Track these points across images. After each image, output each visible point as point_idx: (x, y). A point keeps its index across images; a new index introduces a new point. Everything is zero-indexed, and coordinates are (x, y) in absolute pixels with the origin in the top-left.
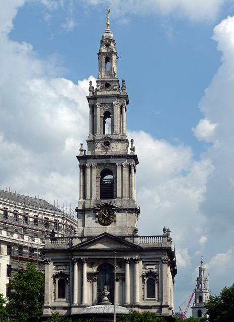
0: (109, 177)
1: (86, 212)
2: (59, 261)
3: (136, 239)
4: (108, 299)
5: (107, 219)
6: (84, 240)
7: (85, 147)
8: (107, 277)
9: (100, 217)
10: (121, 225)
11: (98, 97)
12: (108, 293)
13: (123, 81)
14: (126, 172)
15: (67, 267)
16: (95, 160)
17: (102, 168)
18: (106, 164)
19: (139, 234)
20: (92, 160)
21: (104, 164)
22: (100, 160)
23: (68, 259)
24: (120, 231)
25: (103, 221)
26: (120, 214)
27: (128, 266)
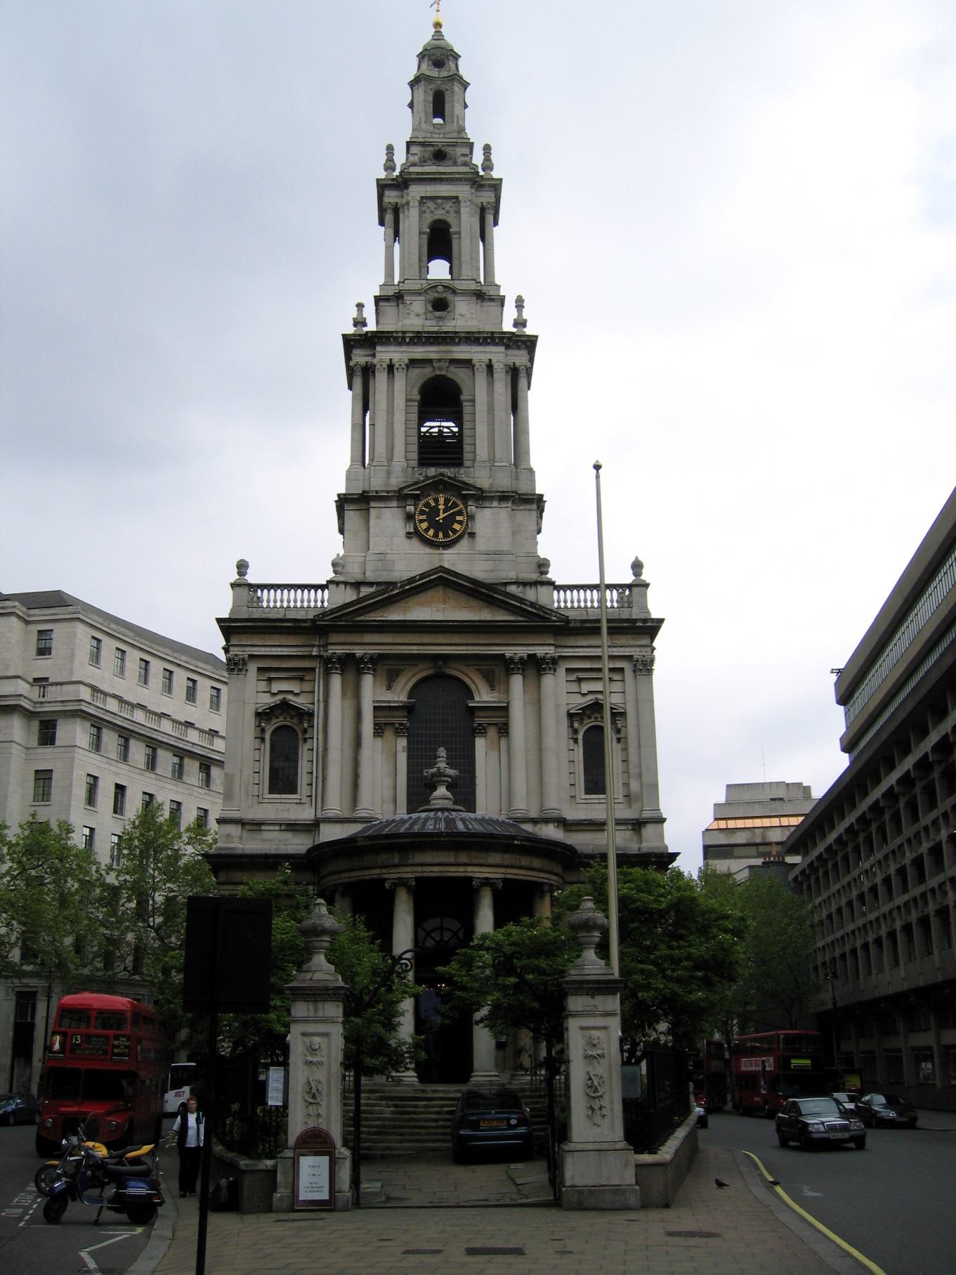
1: (372, 504)
2: (275, 664)
3: (543, 591)
4: (448, 794)
5: (445, 527)
6: (365, 591)
7: (370, 314)
9: (422, 521)
11: (413, 180)
12: (451, 772)
13: (487, 149)
15: (307, 686)
16: (404, 348)
17: (427, 372)
18: (440, 360)
19: (553, 575)
20: (392, 348)
21: (430, 361)
22: (421, 349)
23: (310, 657)
24: (488, 565)
25: (431, 532)
26: (487, 512)
27: (517, 682)
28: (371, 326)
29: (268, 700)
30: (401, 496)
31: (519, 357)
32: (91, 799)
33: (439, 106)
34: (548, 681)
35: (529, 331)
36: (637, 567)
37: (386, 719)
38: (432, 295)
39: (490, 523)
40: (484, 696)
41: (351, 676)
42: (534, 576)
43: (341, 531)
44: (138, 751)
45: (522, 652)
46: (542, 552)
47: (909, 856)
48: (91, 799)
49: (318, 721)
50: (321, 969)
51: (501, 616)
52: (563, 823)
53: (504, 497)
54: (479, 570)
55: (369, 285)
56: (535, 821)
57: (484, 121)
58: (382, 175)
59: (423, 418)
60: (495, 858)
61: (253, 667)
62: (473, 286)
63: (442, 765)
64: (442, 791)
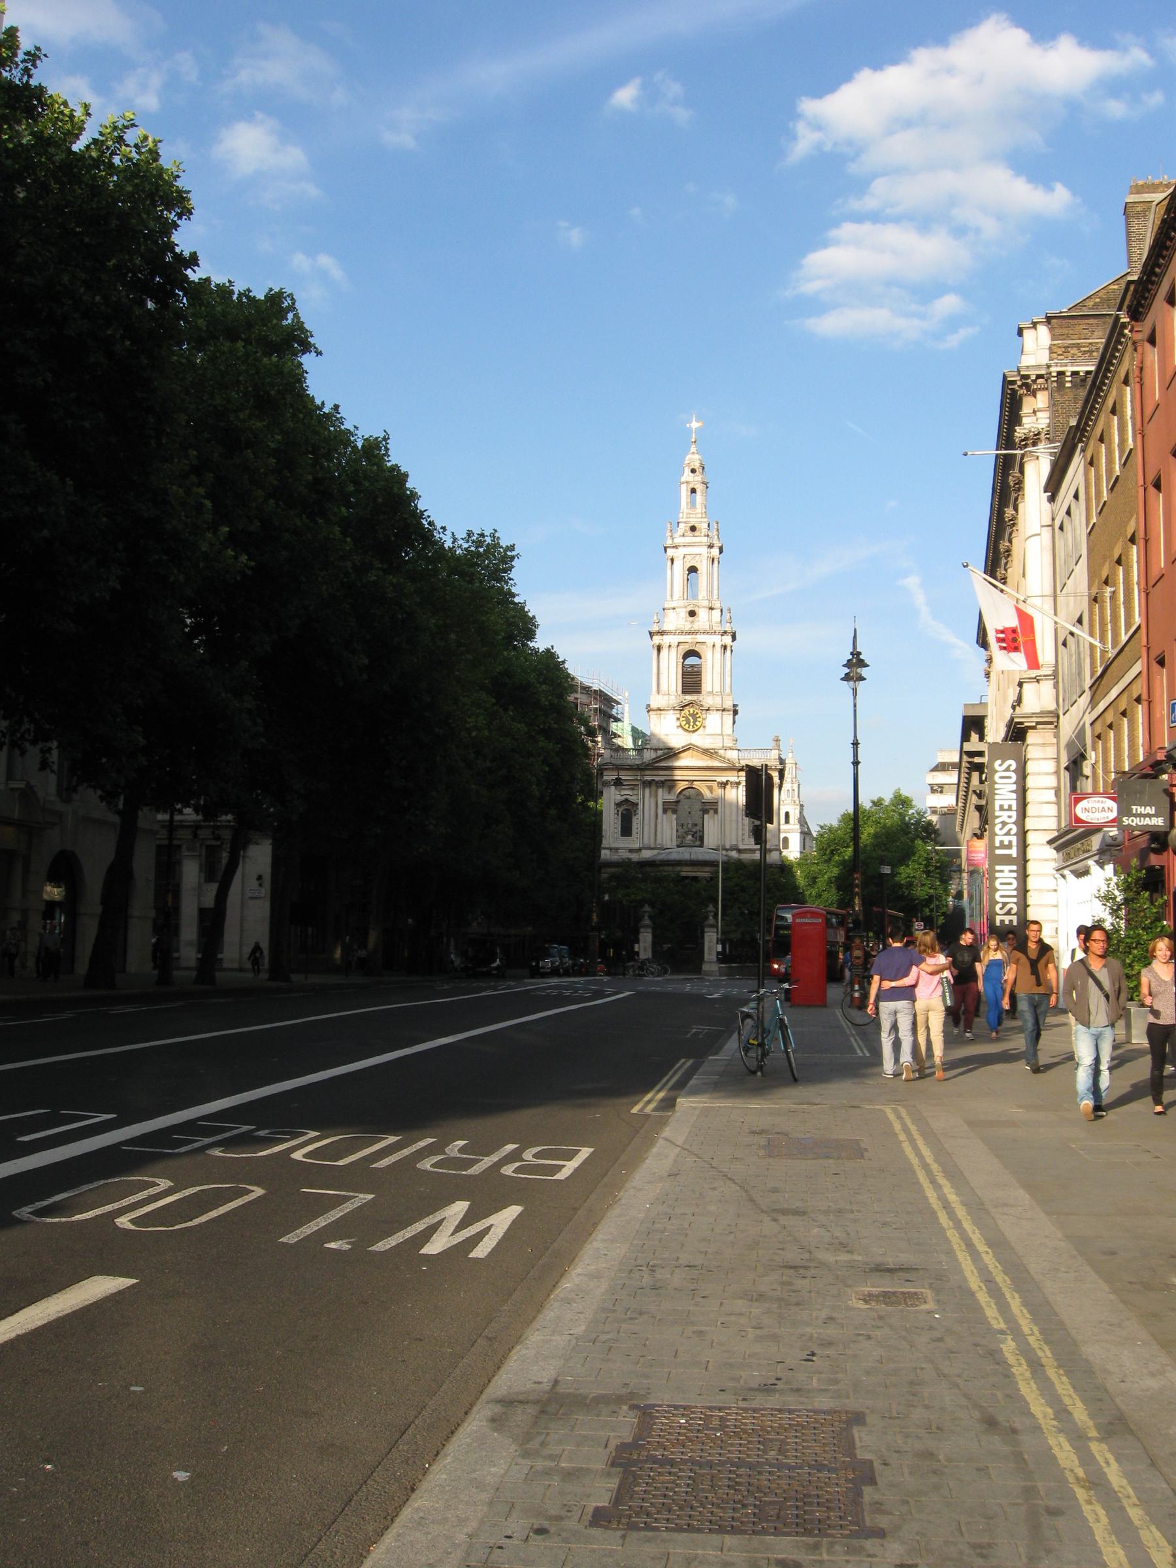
0: (692, 660)
29: (619, 798)
30: (674, 709)
38: (689, 609)
41: (654, 788)
45: (724, 780)
49: (640, 807)
50: (647, 921)
51: (716, 764)
52: (740, 851)
56: (727, 850)
60: (707, 869)
62: (706, 603)
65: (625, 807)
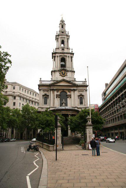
5: (64, 74)
7: (55, 50)
8: (64, 96)
10: (69, 77)
13: (68, 32)
14: (70, 58)
23: (49, 89)
26: (69, 73)
27: (72, 92)
28: (55, 52)
29: (44, 94)
30: (59, 71)
31: (72, 55)
32: (20, 106)
33: (62, 27)
34: (75, 92)
35: (73, 52)
36: (85, 79)
37: (57, 96)
39: (69, 74)
40: (68, 93)
41: (53, 91)
42: (74, 80)
43: (52, 75)
44: (25, 100)
45: (73, 89)
46: (75, 78)
47: (112, 112)
48: (20, 106)
49: (50, 96)
52: (78, 108)
53: (70, 71)
54: (68, 79)
55: (55, 47)
57: (67, 28)
58: (56, 34)
59: (61, 62)
61: (42, 90)
62: (67, 47)
63: (64, 101)
64: (64, 104)
65: (45, 97)
